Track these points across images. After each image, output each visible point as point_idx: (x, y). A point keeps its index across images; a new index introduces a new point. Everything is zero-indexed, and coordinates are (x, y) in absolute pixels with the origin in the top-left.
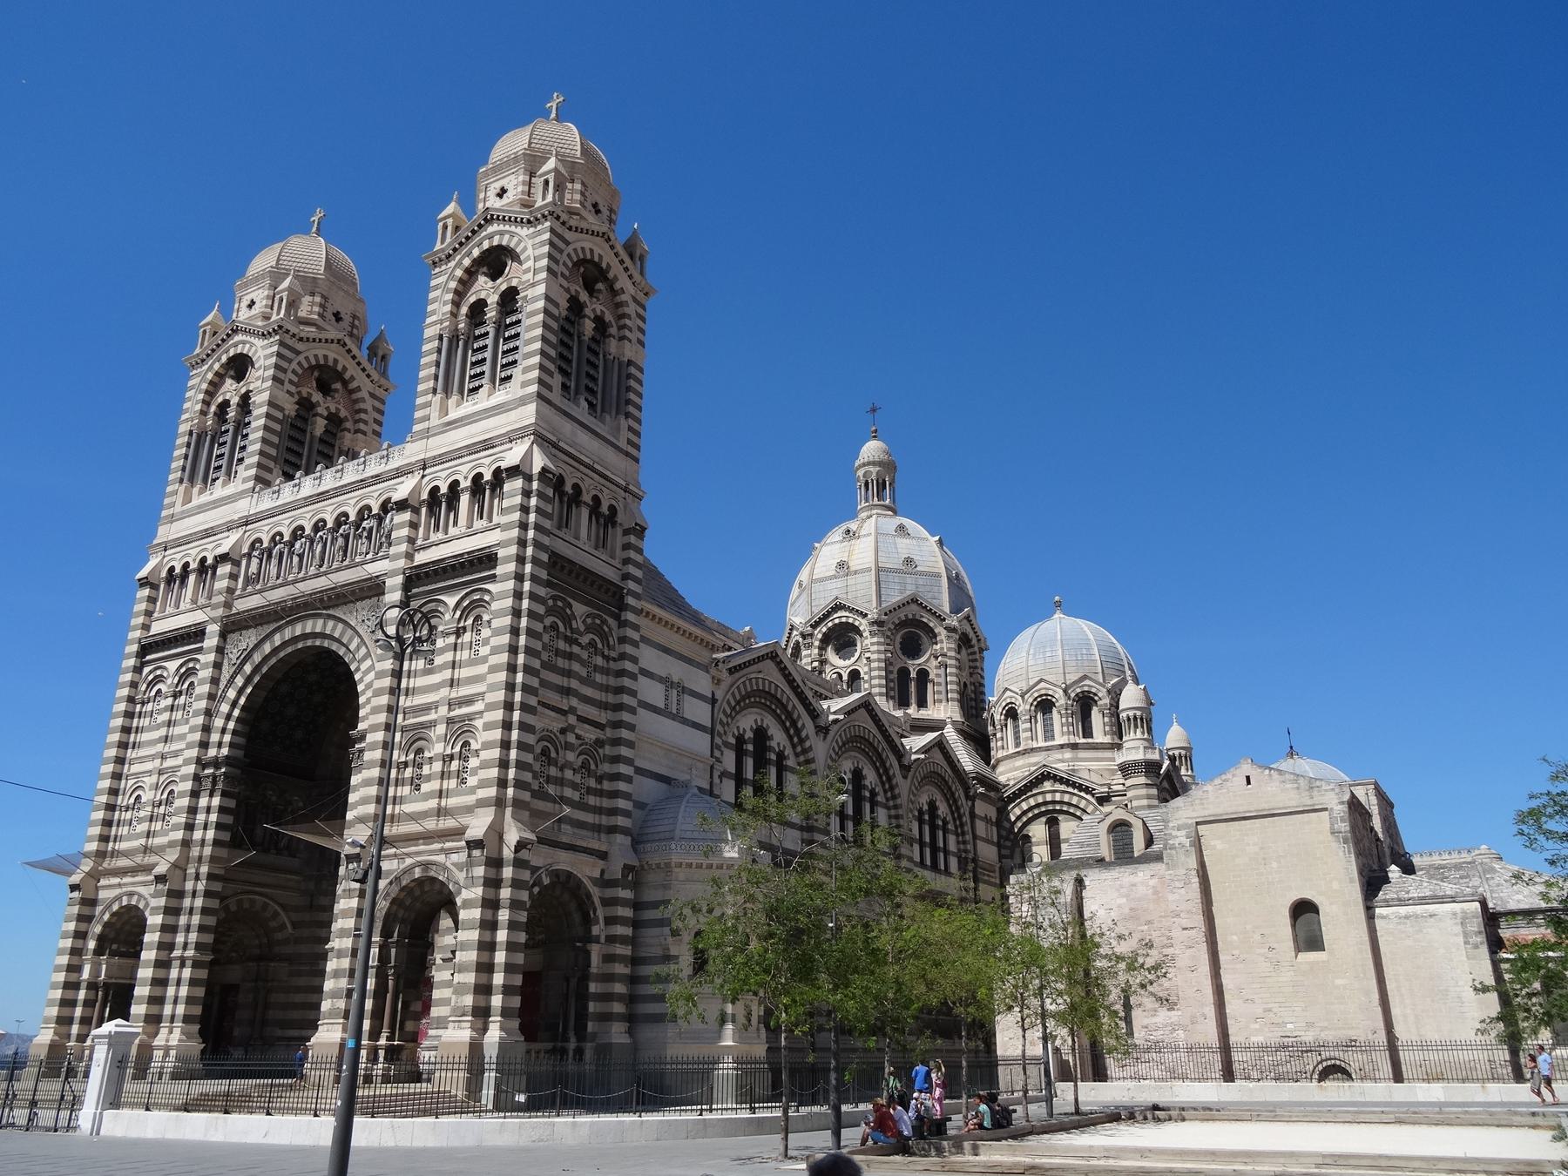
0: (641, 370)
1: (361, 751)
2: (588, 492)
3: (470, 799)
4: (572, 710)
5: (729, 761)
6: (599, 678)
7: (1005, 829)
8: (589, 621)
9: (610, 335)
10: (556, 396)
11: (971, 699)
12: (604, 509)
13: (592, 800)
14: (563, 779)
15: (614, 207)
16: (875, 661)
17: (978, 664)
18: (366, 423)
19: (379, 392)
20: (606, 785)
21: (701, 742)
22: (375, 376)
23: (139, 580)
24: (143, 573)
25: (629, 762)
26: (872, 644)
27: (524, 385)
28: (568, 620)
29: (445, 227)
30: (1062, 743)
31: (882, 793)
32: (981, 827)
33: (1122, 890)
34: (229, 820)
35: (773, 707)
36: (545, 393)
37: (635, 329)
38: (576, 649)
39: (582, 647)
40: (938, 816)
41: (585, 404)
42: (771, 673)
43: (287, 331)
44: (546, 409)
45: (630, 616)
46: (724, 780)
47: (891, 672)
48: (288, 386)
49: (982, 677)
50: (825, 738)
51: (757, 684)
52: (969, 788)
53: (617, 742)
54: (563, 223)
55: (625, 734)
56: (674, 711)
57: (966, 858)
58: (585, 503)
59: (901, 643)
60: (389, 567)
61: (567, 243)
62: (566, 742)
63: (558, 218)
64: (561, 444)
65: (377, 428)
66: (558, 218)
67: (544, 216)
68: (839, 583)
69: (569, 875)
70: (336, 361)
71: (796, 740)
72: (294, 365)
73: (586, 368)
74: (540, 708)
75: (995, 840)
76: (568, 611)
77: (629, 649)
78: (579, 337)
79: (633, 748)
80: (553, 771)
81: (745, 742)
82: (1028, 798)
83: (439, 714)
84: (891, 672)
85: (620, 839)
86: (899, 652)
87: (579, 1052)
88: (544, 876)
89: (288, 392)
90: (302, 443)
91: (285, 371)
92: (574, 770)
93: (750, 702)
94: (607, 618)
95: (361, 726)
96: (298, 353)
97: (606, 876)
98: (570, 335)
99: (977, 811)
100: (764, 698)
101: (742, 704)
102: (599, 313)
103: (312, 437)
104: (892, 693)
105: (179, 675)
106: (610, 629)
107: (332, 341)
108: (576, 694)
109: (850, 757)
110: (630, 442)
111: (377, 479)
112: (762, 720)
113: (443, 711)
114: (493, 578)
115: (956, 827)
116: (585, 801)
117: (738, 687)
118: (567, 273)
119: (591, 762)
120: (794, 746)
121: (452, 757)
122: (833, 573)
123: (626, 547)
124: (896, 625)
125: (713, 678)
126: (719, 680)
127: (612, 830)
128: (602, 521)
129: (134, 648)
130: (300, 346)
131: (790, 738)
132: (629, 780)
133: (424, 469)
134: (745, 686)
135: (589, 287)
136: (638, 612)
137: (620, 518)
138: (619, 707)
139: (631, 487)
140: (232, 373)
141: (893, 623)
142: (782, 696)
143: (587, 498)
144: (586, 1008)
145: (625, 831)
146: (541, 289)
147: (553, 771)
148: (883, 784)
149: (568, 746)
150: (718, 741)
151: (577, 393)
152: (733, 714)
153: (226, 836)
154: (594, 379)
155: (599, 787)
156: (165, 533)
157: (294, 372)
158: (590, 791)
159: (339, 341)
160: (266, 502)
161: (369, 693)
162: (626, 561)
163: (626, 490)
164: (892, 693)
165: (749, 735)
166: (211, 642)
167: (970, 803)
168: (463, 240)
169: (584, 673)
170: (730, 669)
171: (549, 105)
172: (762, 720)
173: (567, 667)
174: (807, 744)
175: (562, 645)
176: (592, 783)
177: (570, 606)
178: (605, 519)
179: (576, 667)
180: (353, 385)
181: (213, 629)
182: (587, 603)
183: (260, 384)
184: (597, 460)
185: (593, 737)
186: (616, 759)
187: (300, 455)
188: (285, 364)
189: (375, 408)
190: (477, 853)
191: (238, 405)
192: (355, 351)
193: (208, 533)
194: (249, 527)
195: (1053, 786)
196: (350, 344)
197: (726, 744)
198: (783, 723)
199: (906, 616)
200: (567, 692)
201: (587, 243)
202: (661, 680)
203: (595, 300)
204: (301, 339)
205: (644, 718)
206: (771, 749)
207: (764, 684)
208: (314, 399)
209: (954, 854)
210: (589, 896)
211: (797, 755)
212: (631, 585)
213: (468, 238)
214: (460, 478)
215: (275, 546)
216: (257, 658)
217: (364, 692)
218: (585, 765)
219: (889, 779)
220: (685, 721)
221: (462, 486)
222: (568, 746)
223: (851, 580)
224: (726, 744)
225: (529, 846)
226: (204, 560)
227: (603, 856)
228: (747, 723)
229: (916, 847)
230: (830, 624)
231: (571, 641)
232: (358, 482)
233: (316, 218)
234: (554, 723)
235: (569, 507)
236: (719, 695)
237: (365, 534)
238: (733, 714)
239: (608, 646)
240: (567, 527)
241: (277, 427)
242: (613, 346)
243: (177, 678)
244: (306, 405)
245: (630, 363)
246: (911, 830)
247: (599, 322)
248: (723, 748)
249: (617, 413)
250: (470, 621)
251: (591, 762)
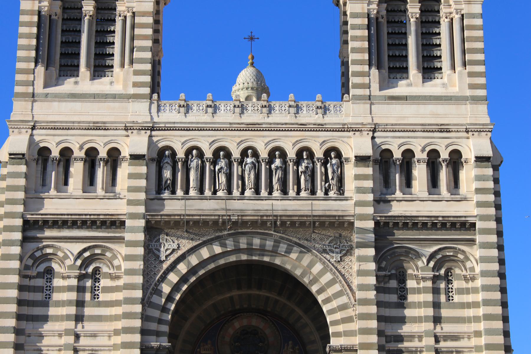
114: (471, 242)
194: (154, 133)
216: (194, 260)
250: (442, 272)
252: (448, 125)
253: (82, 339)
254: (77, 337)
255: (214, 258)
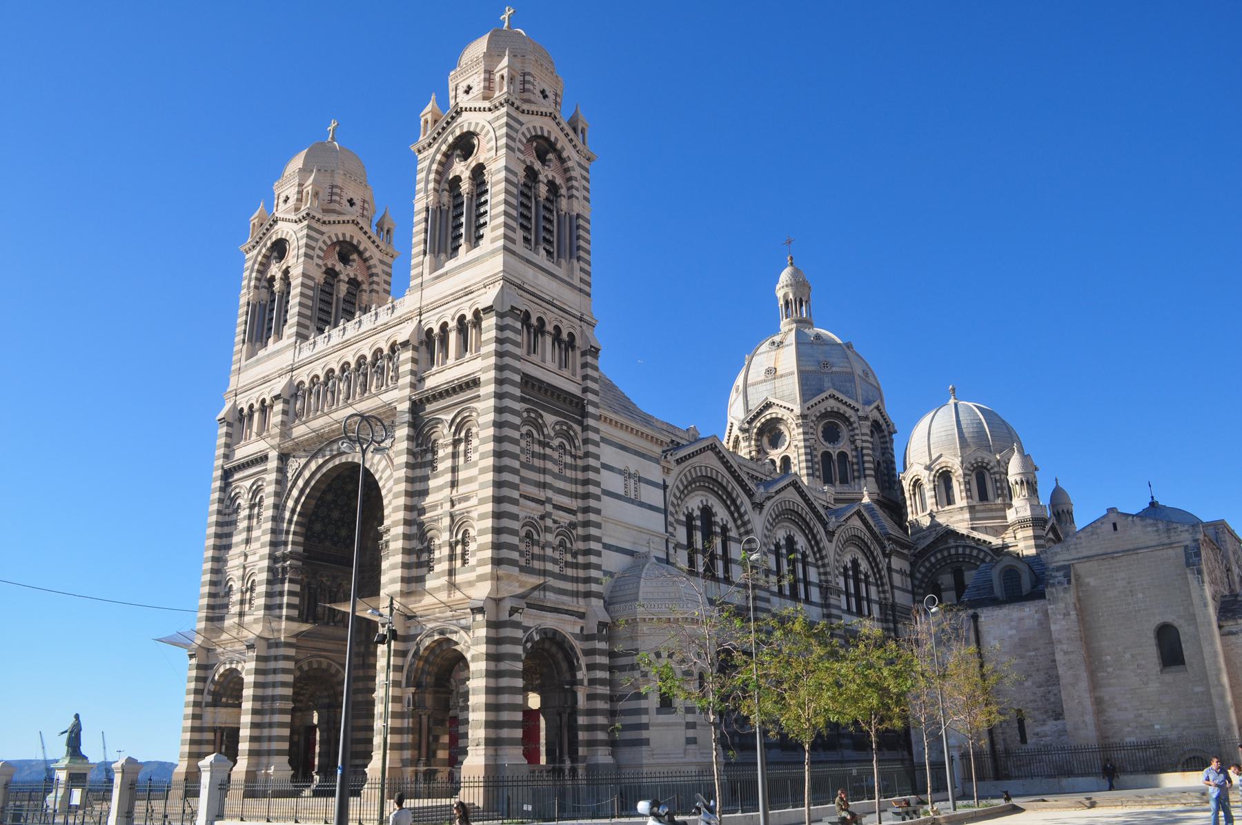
0: (588, 221)
1: (387, 542)
2: (550, 323)
3: (472, 576)
4: (549, 500)
5: (681, 534)
6: (569, 473)
7: (917, 579)
8: (558, 427)
9: (561, 195)
10: (520, 247)
11: (884, 475)
12: (565, 336)
13: (570, 572)
14: (545, 555)
15: (558, 92)
16: (801, 448)
17: (889, 445)
18: (378, 284)
19: (387, 259)
20: (581, 559)
21: (656, 522)
22: (383, 246)
23: (219, 420)
24: (221, 415)
25: (598, 539)
26: (799, 434)
27: (493, 240)
28: (540, 428)
29: (426, 122)
30: (961, 506)
31: (812, 555)
32: (897, 579)
33: (1012, 623)
34: (296, 601)
35: (716, 489)
36: (510, 245)
37: (581, 188)
38: (548, 451)
39: (553, 449)
40: (861, 572)
41: (543, 252)
42: (710, 460)
43: (313, 217)
44: (513, 260)
45: (591, 422)
46: (678, 550)
47: (816, 456)
48: (316, 260)
49: (893, 456)
50: (760, 513)
51: (701, 470)
52: (885, 547)
53: (586, 524)
54: (517, 108)
55: (593, 517)
56: (633, 497)
57: (886, 605)
58: (548, 332)
59: (822, 432)
60: (398, 396)
61: (521, 124)
62: (545, 526)
63: (512, 104)
64: (526, 286)
65: (387, 287)
66: (512, 104)
67: (501, 104)
68: (768, 386)
69: (555, 632)
70: (352, 237)
71: (736, 515)
72: (320, 243)
73: (543, 223)
74: (522, 501)
75: (910, 588)
76: (540, 421)
77: (592, 448)
78: (536, 199)
79: (600, 528)
80: (536, 550)
81: (694, 519)
82: (936, 553)
83: (444, 509)
84: (816, 456)
85: (594, 601)
86: (822, 440)
87: (574, 771)
88: (534, 634)
89: (317, 265)
90: (330, 304)
91: (313, 249)
92: (553, 548)
93: (696, 486)
94: (572, 424)
95: (387, 522)
96: (322, 233)
97: (585, 632)
98: (529, 198)
99: (893, 566)
100: (709, 483)
101: (689, 488)
102: (550, 178)
103: (338, 299)
104: (817, 473)
105: (252, 491)
106: (576, 434)
107: (348, 222)
108: (551, 487)
109: (783, 527)
110: (581, 280)
111: (387, 326)
112: (707, 500)
113: (447, 506)
115: (876, 579)
116: (564, 572)
117: (685, 475)
118: (523, 148)
119: (567, 541)
120: (735, 521)
121: (457, 543)
122: (763, 378)
123: (584, 365)
124: (818, 418)
125: (664, 467)
126: (668, 469)
127: (588, 595)
128: (563, 346)
129: (219, 473)
130: (324, 228)
131: (732, 514)
132: (598, 554)
133: (420, 315)
134: (690, 473)
135: (542, 158)
136: (598, 418)
137: (578, 342)
138: (586, 496)
139: (585, 317)
140: (275, 254)
141: (815, 415)
142: (722, 480)
143: (549, 328)
144: (576, 736)
145: (598, 595)
146: (502, 162)
147: (536, 550)
148: (812, 548)
149: (547, 530)
150: (670, 519)
151: (537, 243)
152: (682, 496)
153: (295, 613)
154: (550, 232)
155: (574, 561)
156: (234, 383)
157: (320, 249)
158: (567, 564)
159: (353, 221)
160: (307, 352)
161: (390, 496)
162: (585, 377)
163: (581, 319)
164: (817, 473)
165: (697, 513)
166: (273, 464)
167: (887, 560)
168: (440, 131)
169: (556, 469)
170: (677, 460)
171: (502, 17)
172: (707, 500)
173: (542, 466)
174: (746, 518)
175: (537, 448)
176: (569, 558)
177: (541, 417)
178: (566, 344)
179: (549, 465)
180: (367, 254)
181: (273, 454)
182: (555, 413)
183: (295, 262)
184: (555, 296)
185: (568, 522)
186: (587, 538)
187: (329, 313)
188: (313, 244)
189: (383, 271)
190: (479, 617)
191: (281, 279)
192: (366, 228)
193: (266, 380)
194: (294, 373)
195: (955, 542)
196: (362, 223)
197: (678, 521)
198: (724, 502)
199: (826, 409)
200: (544, 486)
201: (537, 122)
202: (620, 472)
203: (546, 167)
204: (324, 223)
205: (607, 505)
206: (716, 523)
207: (706, 471)
208: (337, 269)
209: (876, 602)
210: (572, 648)
211: (738, 527)
212: (590, 396)
213: (444, 129)
214: (448, 320)
215: (314, 385)
216: (307, 474)
217: (386, 495)
218: (562, 544)
219: (817, 543)
220: (642, 504)
221: (450, 326)
222: (547, 530)
223: (778, 382)
224: (678, 521)
225: (521, 611)
226: (263, 401)
227: (582, 616)
228: (694, 503)
229: (843, 598)
230: (763, 420)
231: (544, 445)
232: (371, 330)
233: (331, 128)
234: (534, 510)
235: (536, 336)
236: (670, 482)
237: (379, 371)
238: (682, 496)
239: (575, 447)
240: (534, 352)
241: (310, 293)
242: (564, 203)
243: (251, 494)
244: (331, 273)
245: (578, 216)
246: (838, 584)
247: (551, 184)
248: (675, 525)
249: (571, 257)
250: (463, 434)
251: (567, 541)
252: (469, 286)
253: (249, 557)
254: (246, 556)
255: (319, 468)
